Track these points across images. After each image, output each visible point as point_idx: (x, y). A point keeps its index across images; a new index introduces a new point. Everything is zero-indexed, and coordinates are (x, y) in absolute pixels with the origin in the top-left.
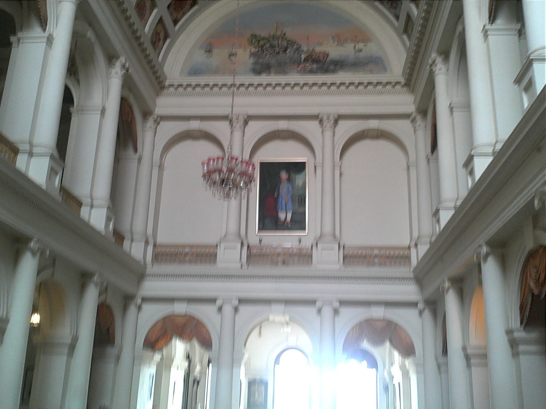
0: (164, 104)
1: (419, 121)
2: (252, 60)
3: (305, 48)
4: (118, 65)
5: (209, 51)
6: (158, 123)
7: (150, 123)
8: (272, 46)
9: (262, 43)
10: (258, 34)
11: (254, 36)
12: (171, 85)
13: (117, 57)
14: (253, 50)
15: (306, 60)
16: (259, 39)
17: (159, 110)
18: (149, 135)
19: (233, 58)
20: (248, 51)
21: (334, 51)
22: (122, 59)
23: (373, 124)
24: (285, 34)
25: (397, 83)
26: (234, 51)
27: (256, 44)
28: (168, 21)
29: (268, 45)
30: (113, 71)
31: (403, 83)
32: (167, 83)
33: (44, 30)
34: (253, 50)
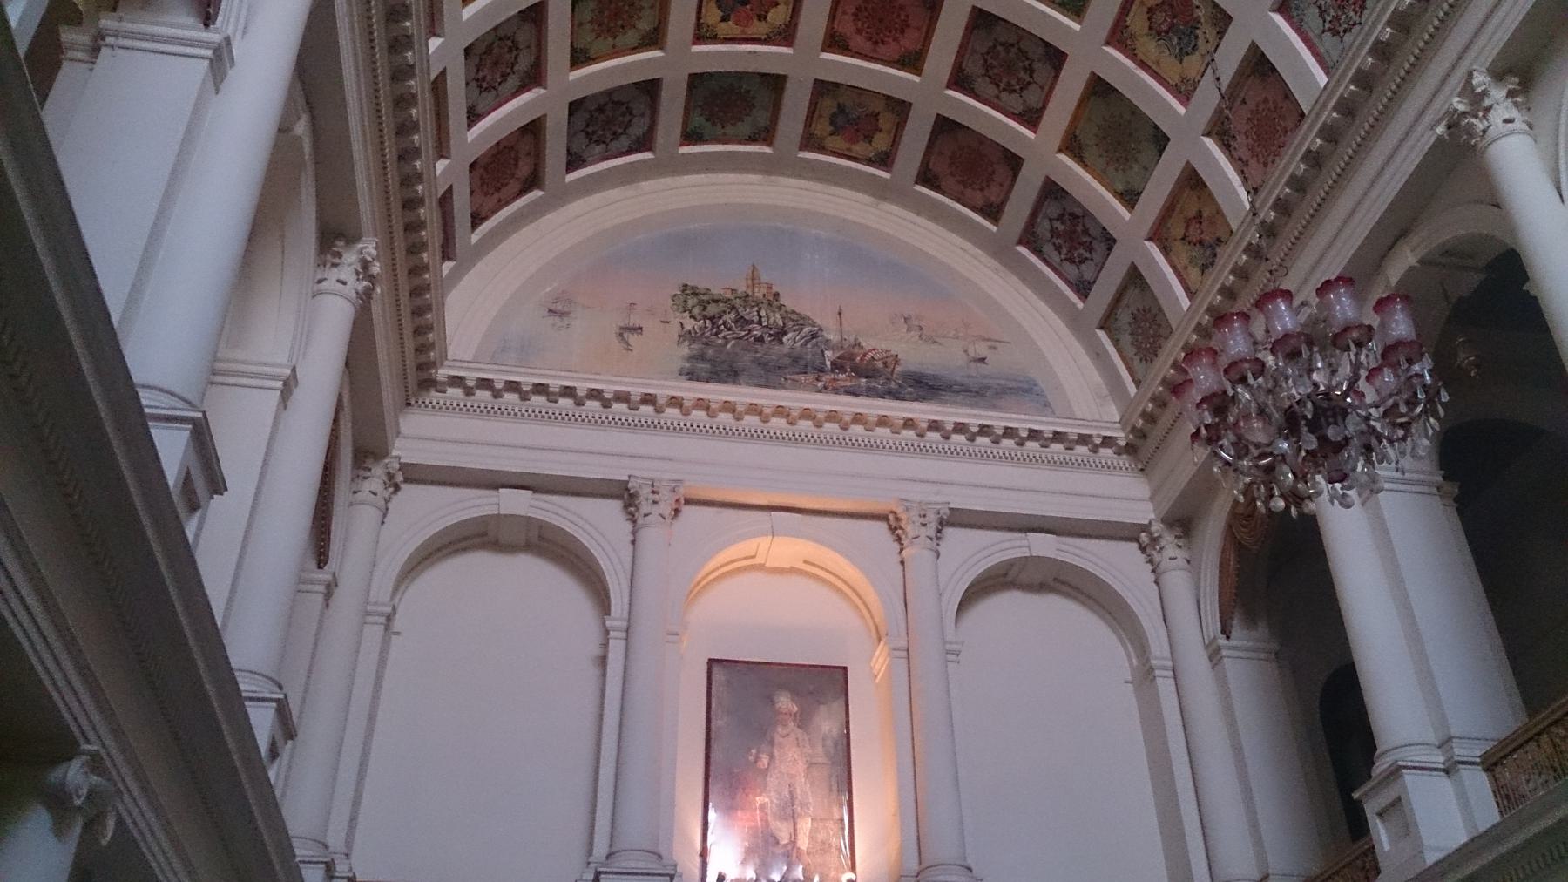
0: (421, 435)
1: (1171, 550)
2: (685, 350)
3: (833, 337)
4: (350, 257)
5: (558, 312)
6: (397, 488)
7: (375, 482)
8: (741, 321)
9: (712, 309)
10: (702, 285)
11: (689, 291)
12: (457, 381)
13: (352, 239)
14: (689, 324)
15: (838, 366)
16: (705, 298)
17: (405, 450)
18: (366, 516)
19: (633, 339)
20: (675, 322)
21: (914, 355)
22: (369, 246)
23: (1043, 545)
24: (776, 295)
25: (1107, 441)
26: (635, 321)
27: (696, 311)
28: (462, 205)
29: (729, 318)
30: (334, 274)
31: (1123, 443)
32: (442, 373)
33: (208, 20)
34: (689, 324)
